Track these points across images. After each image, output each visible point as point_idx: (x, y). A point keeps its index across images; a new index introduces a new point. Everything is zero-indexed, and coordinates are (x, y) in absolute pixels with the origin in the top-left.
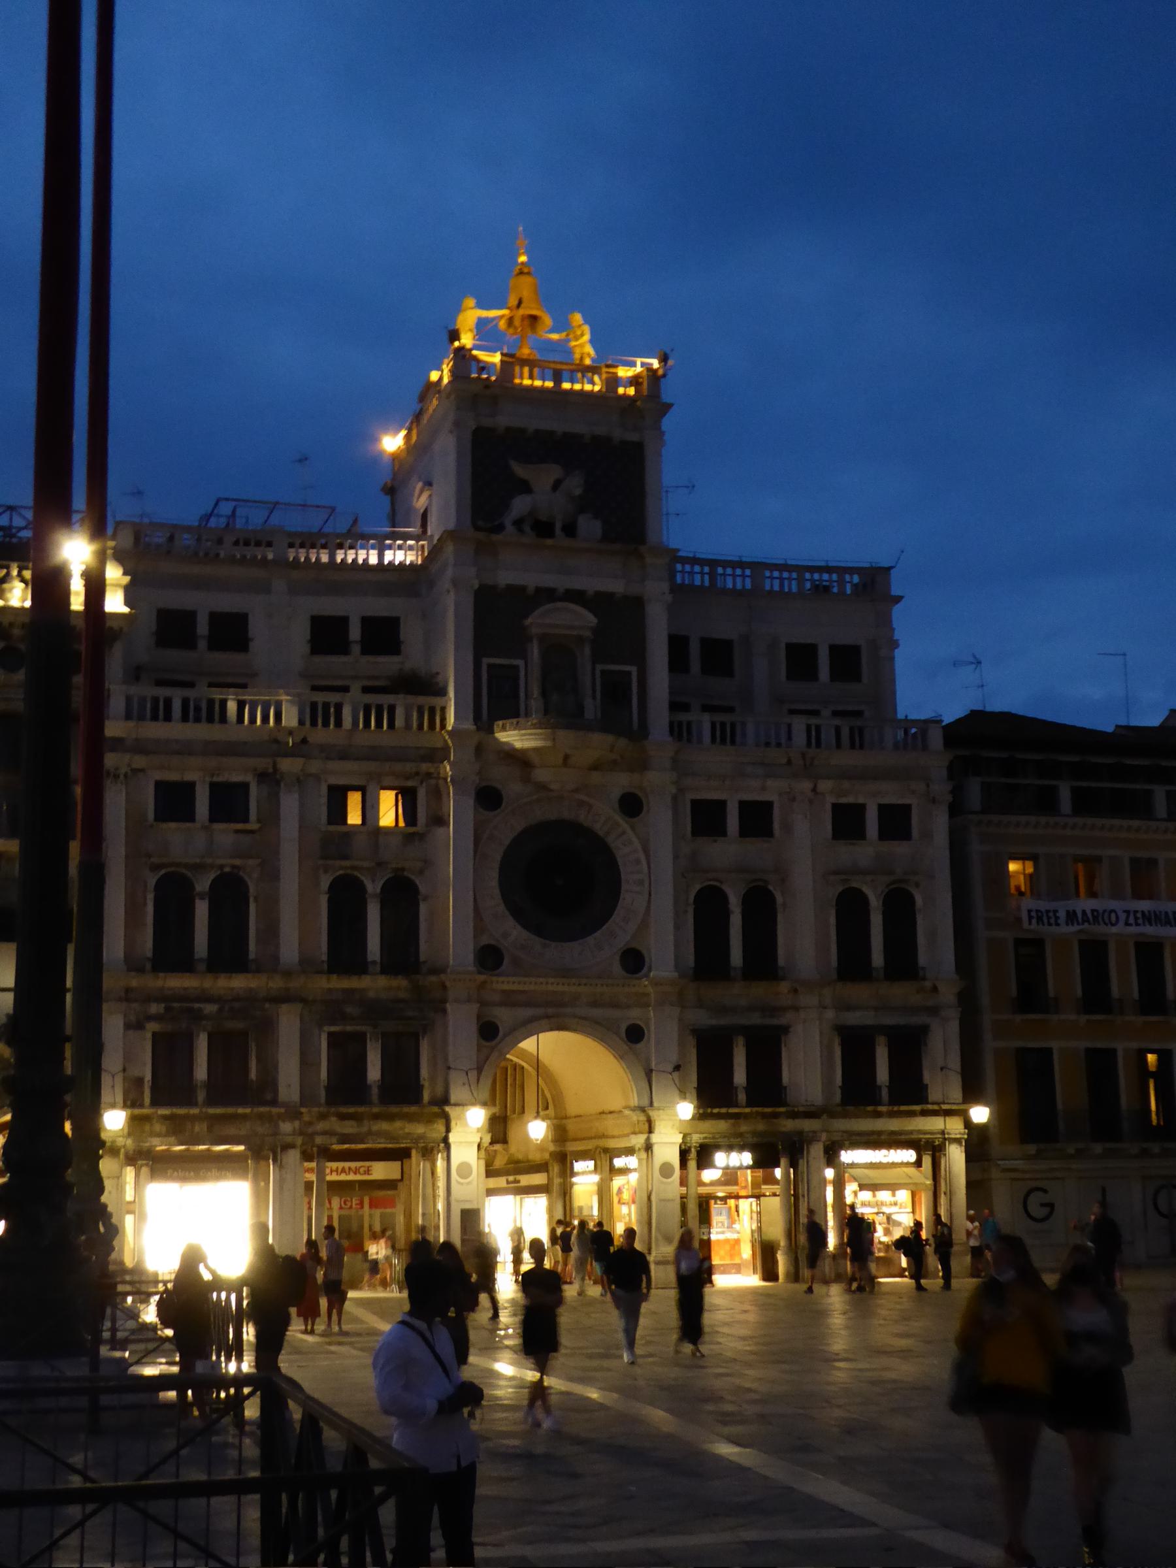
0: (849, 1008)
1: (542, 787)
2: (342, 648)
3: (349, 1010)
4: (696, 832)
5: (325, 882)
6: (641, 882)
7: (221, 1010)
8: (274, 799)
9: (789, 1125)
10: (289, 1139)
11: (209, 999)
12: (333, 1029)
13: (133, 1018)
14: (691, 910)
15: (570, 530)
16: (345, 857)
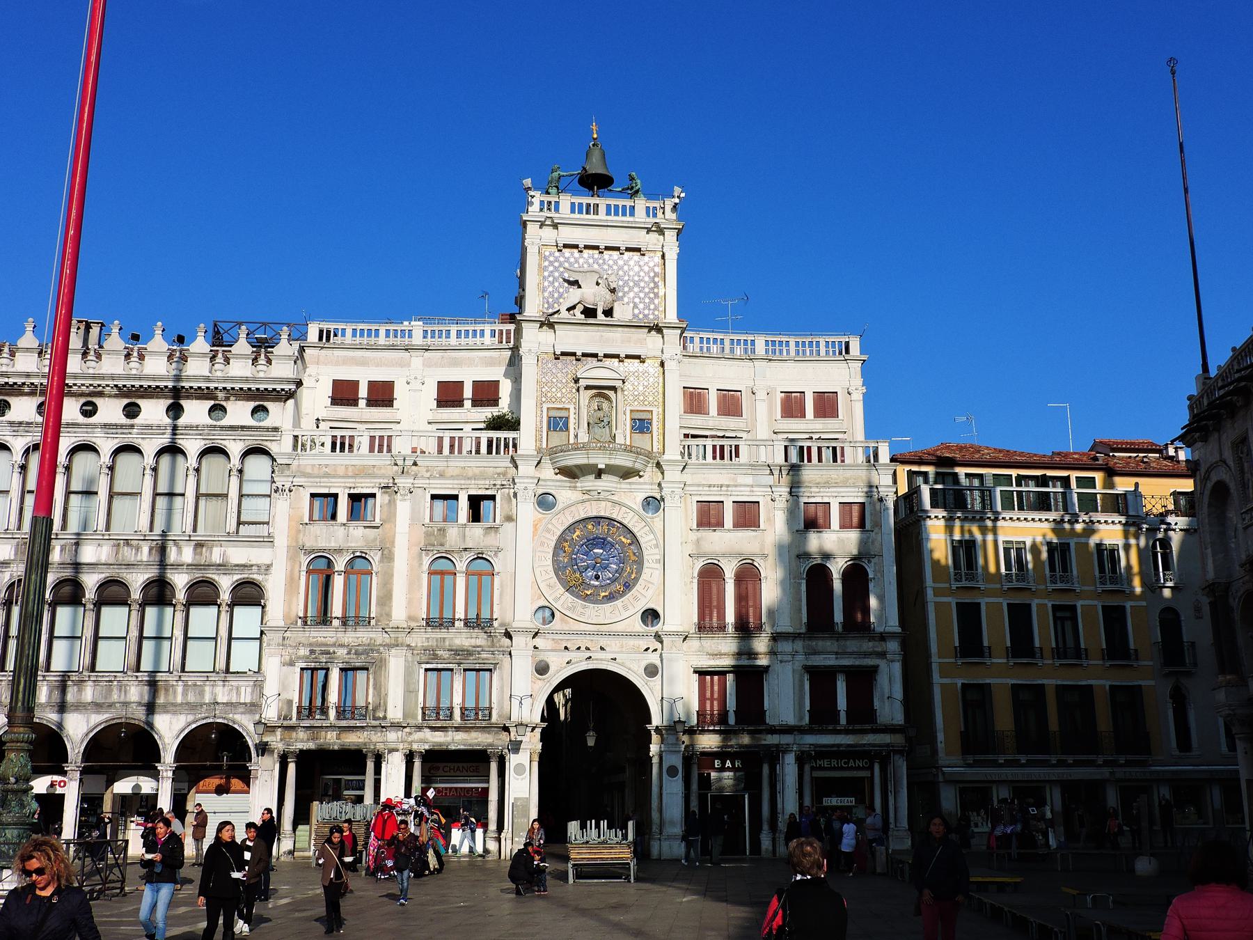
0: (815, 653)
1: (587, 492)
2: (459, 403)
3: (439, 653)
4: (701, 524)
5: (427, 561)
6: (658, 561)
7: (349, 653)
8: (392, 503)
9: (772, 740)
10: (392, 746)
11: (342, 646)
12: (429, 666)
13: (288, 658)
14: (696, 581)
15: (609, 313)
16: (442, 545)
